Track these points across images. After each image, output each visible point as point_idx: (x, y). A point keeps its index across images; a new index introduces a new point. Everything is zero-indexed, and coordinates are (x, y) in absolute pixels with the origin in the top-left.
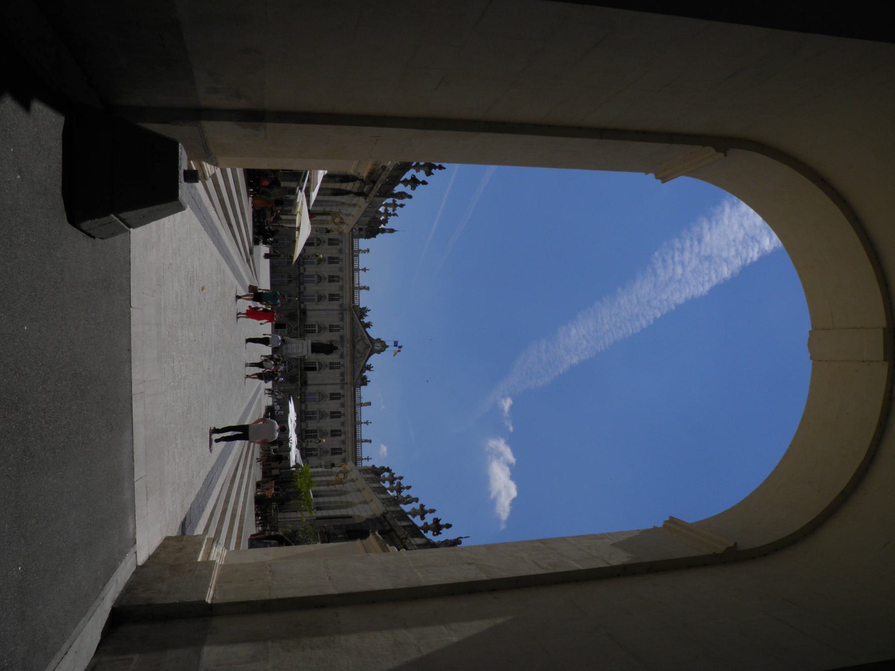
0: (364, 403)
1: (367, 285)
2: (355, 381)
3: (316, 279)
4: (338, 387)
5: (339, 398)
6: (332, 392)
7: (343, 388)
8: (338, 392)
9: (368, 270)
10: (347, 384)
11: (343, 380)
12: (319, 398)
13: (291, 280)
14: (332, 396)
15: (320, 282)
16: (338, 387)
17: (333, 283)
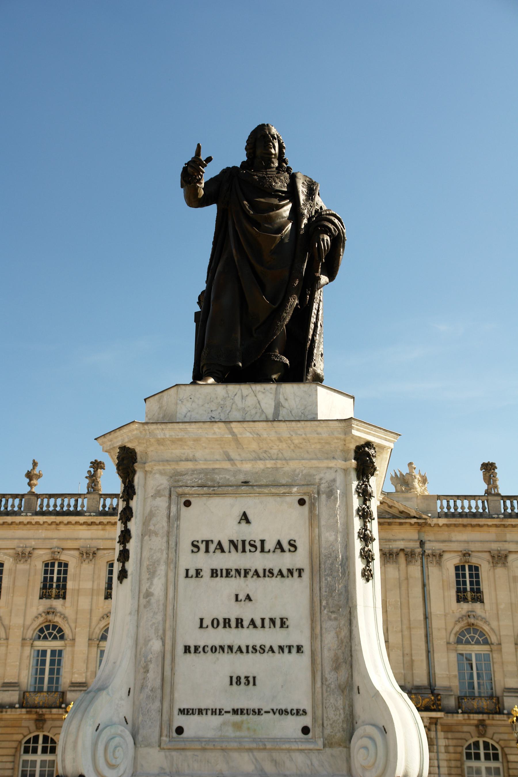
0: (485, 487)
1: (87, 467)
2: (413, 513)
3: (50, 645)
4: (433, 571)
5: (475, 570)
6: (453, 593)
7: (438, 556)
8: (452, 572)
9: (35, 464)
10: (422, 543)
11: (410, 555)
12: (478, 643)
13: (46, 738)
14: (469, 595)
15: (60, 630)
16: (433, 571)
17: (70, 585)
